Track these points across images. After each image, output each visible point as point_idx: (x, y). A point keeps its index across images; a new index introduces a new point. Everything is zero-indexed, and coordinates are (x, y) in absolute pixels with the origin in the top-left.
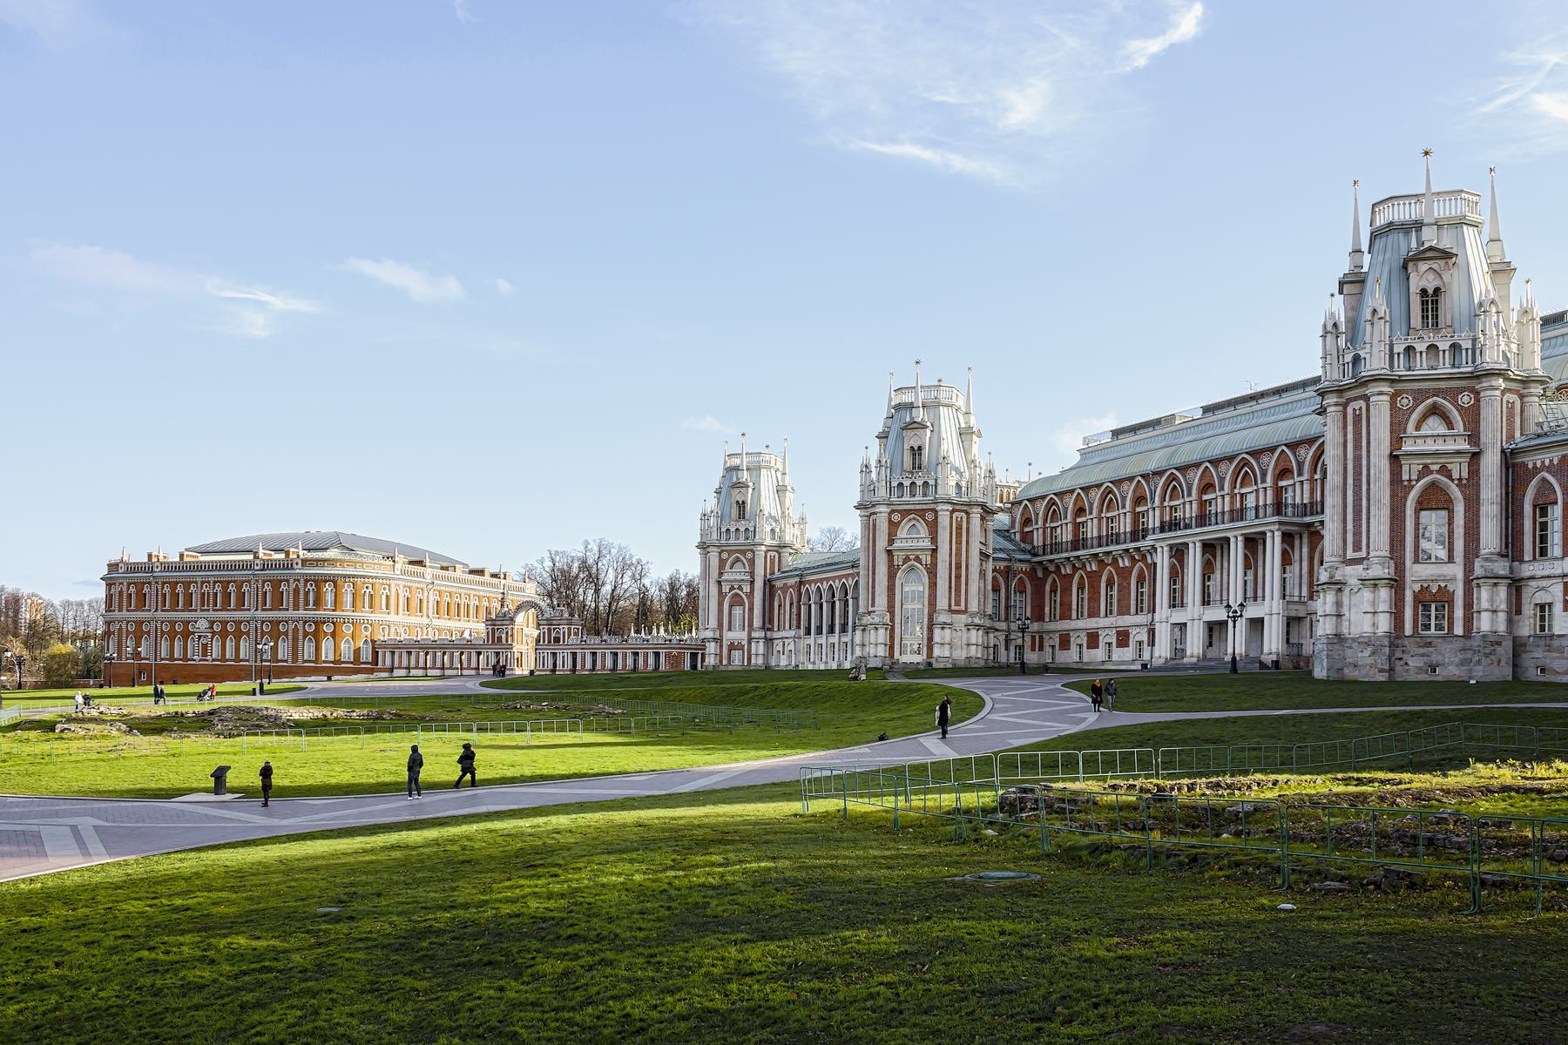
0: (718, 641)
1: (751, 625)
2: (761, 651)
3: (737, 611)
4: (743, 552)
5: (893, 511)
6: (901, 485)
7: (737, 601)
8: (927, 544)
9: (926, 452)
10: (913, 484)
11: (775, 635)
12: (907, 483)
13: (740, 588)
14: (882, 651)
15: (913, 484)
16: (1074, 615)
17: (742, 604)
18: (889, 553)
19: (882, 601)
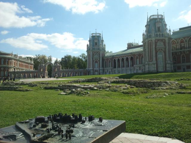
0: (93, 70)
1: (100, 67)
2: (102, 72)
3: (96, 64)
4: (98, 52)
5: (155, 40)
6: (157, 34)
7: (96, 62)
8: (163, 46)
9: (161, 28)
10: (160, 34)
11: (105, 69)
12: (158, 34)
13: (97, 59)
14: (156, 69)
15: (160, 34)
16: (181, 62)
17: (97, 62)
18: (156, 48)
19: (154, 58)
